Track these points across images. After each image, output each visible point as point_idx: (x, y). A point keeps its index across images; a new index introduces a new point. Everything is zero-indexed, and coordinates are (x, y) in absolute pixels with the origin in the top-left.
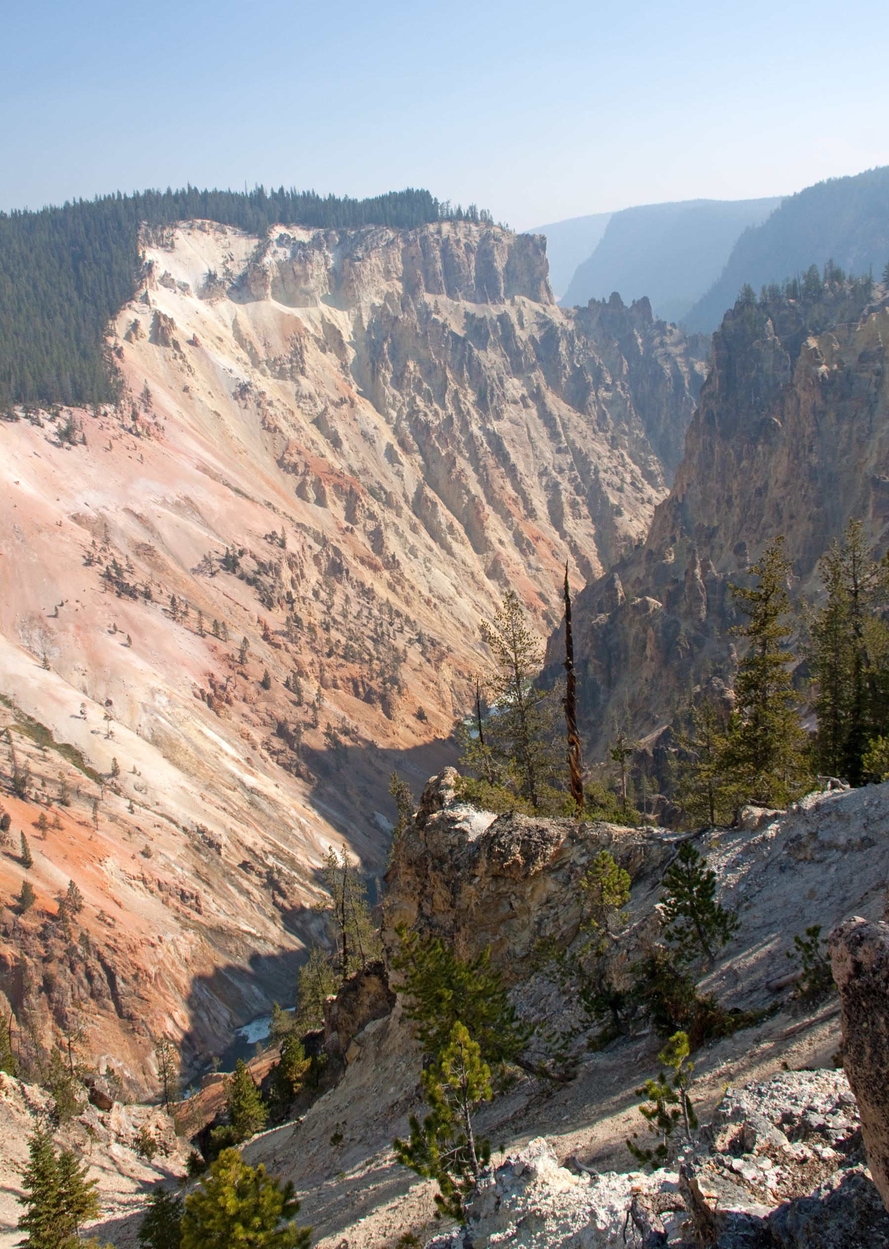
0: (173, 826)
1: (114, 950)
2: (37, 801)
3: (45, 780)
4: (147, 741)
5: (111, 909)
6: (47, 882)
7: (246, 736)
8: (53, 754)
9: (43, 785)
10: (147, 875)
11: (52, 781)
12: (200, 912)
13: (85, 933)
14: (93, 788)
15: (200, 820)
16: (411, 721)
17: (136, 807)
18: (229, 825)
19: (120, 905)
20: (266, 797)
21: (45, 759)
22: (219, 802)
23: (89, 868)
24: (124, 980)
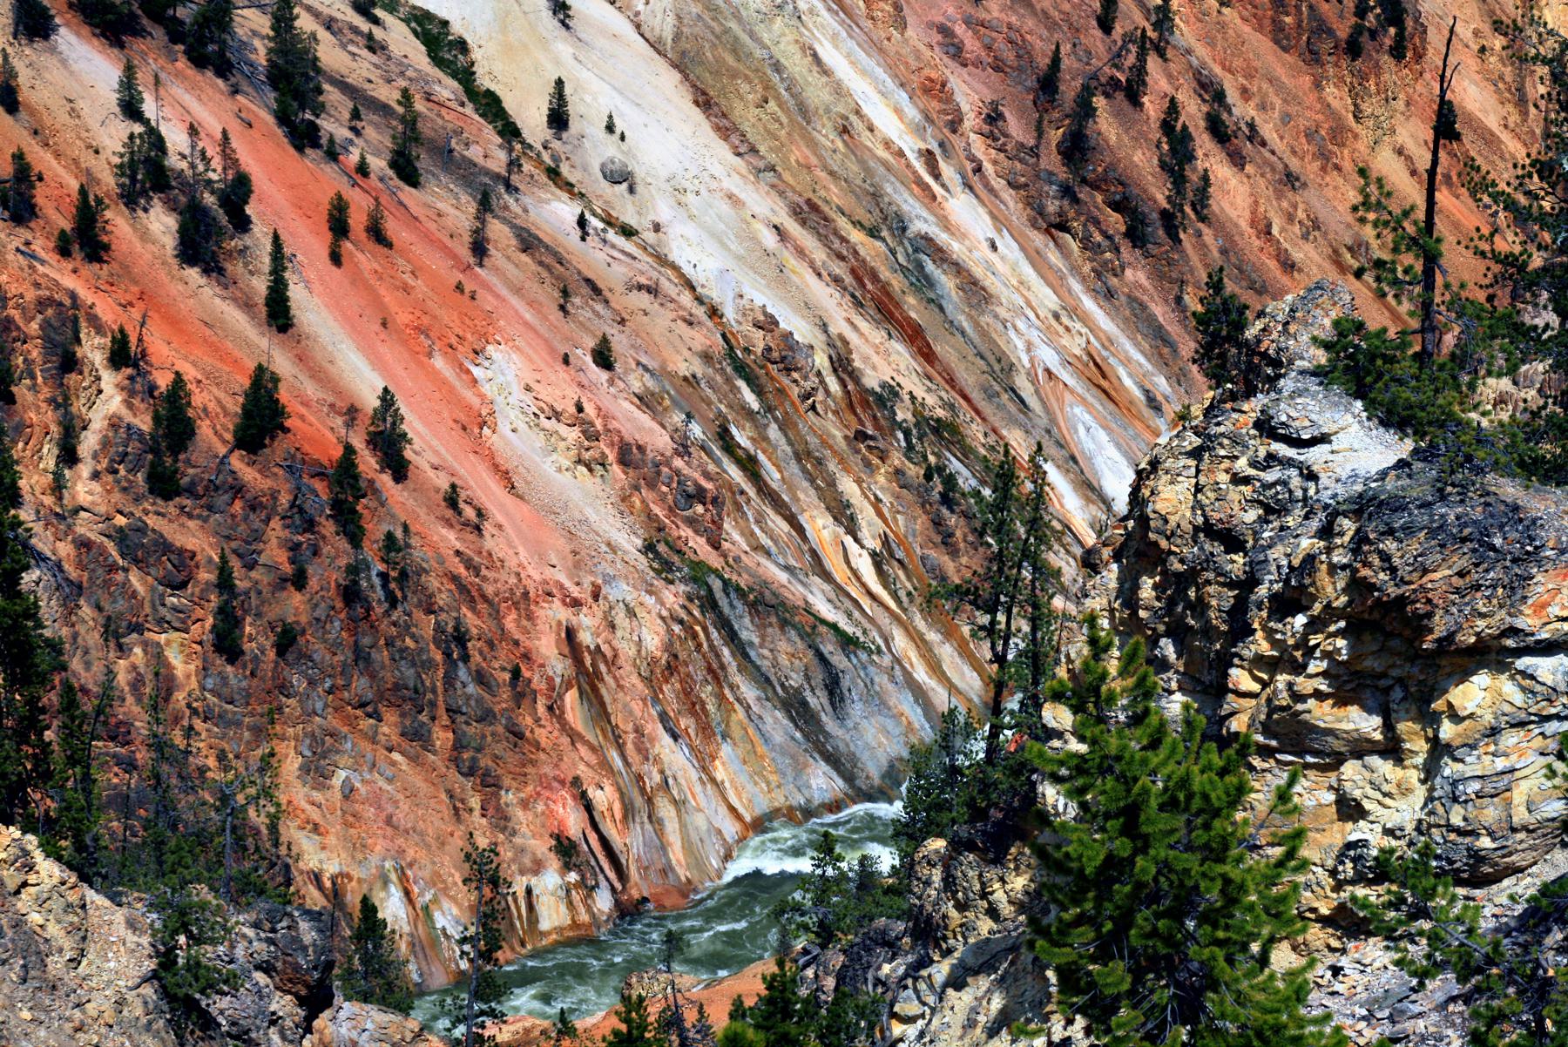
0: (686, 299)
1: (467, 594)
2: (332, 155)
3: (362, 104)
4: (656, 46)
5: (483, 488)
6: (319, 374)
7: (935, 90)
8: (398, 36)
9: (356, 115)
10: (590, 410)
11: (384, 109)
12: (716, 545)
13: (399, 534)
14: (487, 150)
15: (762, 297)
16: (1415, 134)
17: (595, 223)
18: (839, 326)
19: (506, 477)
20: (958, 269)
21: (373, 46)
22: (819, 254)
23: (439, 362)
24: (481, 678)
